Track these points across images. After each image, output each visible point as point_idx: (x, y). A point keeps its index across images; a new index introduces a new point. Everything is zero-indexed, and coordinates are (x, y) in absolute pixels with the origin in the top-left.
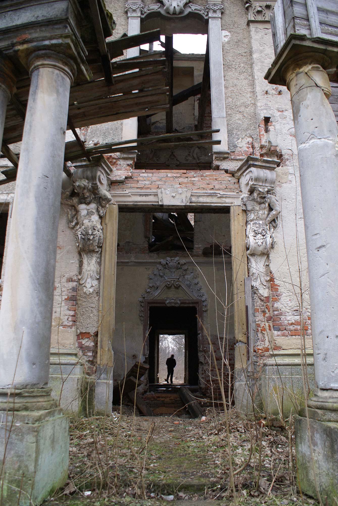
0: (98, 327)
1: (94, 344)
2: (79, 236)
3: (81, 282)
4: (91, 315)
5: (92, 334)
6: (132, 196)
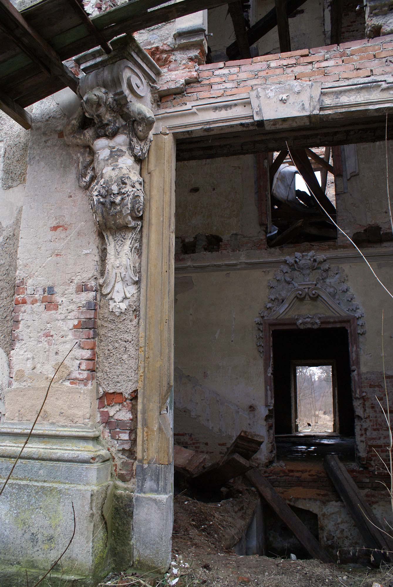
0: (137, 381)
1: (131, 417)
2: (95, 198)
3: (105, 291)
4: (125, 357)
5: (127, 396)
6: (200, 113)
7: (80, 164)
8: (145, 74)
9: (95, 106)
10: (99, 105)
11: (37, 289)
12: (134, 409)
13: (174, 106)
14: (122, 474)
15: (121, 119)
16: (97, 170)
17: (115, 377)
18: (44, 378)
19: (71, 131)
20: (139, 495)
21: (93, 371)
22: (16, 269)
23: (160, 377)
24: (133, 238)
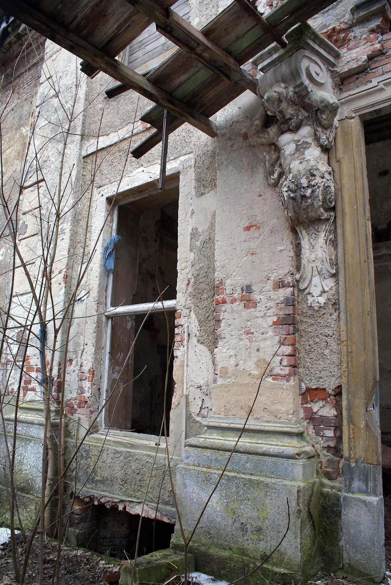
0: (340, 377)
1: (336, 413)
2: (285, 194)
3: (302, 286)
4: (327, 352)
5: (330, 392)
7: (267, 163)
8: (323, 59)
9: (276, 103)
10: (280, 101)
11: (236, 289)
12: (339, 405)
13: (357, 87)
14: (328, 472)
15: (303, 111)
16: (284, 166)
17: (318, 372)
18: (247, 374)
19: (255, 132)
20: (346, 494)
21: (294, 366)
22: (214, 271)
23: (365, 372)
24: (327, 230)
